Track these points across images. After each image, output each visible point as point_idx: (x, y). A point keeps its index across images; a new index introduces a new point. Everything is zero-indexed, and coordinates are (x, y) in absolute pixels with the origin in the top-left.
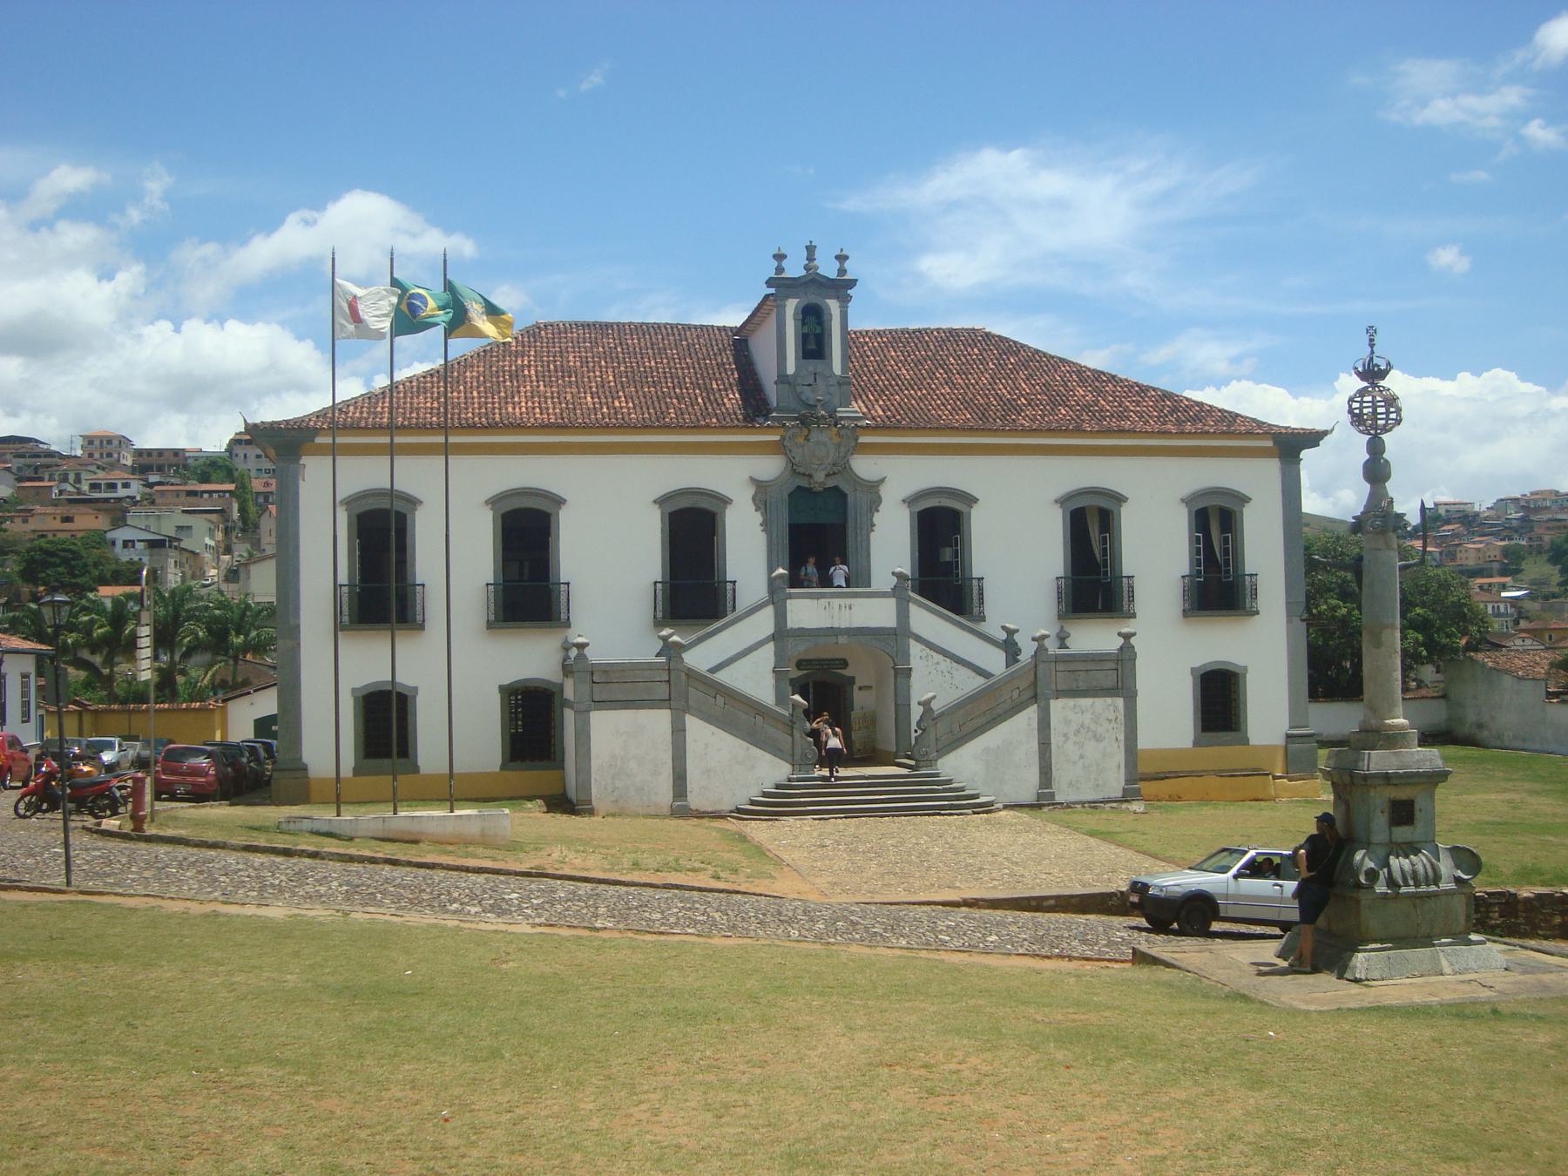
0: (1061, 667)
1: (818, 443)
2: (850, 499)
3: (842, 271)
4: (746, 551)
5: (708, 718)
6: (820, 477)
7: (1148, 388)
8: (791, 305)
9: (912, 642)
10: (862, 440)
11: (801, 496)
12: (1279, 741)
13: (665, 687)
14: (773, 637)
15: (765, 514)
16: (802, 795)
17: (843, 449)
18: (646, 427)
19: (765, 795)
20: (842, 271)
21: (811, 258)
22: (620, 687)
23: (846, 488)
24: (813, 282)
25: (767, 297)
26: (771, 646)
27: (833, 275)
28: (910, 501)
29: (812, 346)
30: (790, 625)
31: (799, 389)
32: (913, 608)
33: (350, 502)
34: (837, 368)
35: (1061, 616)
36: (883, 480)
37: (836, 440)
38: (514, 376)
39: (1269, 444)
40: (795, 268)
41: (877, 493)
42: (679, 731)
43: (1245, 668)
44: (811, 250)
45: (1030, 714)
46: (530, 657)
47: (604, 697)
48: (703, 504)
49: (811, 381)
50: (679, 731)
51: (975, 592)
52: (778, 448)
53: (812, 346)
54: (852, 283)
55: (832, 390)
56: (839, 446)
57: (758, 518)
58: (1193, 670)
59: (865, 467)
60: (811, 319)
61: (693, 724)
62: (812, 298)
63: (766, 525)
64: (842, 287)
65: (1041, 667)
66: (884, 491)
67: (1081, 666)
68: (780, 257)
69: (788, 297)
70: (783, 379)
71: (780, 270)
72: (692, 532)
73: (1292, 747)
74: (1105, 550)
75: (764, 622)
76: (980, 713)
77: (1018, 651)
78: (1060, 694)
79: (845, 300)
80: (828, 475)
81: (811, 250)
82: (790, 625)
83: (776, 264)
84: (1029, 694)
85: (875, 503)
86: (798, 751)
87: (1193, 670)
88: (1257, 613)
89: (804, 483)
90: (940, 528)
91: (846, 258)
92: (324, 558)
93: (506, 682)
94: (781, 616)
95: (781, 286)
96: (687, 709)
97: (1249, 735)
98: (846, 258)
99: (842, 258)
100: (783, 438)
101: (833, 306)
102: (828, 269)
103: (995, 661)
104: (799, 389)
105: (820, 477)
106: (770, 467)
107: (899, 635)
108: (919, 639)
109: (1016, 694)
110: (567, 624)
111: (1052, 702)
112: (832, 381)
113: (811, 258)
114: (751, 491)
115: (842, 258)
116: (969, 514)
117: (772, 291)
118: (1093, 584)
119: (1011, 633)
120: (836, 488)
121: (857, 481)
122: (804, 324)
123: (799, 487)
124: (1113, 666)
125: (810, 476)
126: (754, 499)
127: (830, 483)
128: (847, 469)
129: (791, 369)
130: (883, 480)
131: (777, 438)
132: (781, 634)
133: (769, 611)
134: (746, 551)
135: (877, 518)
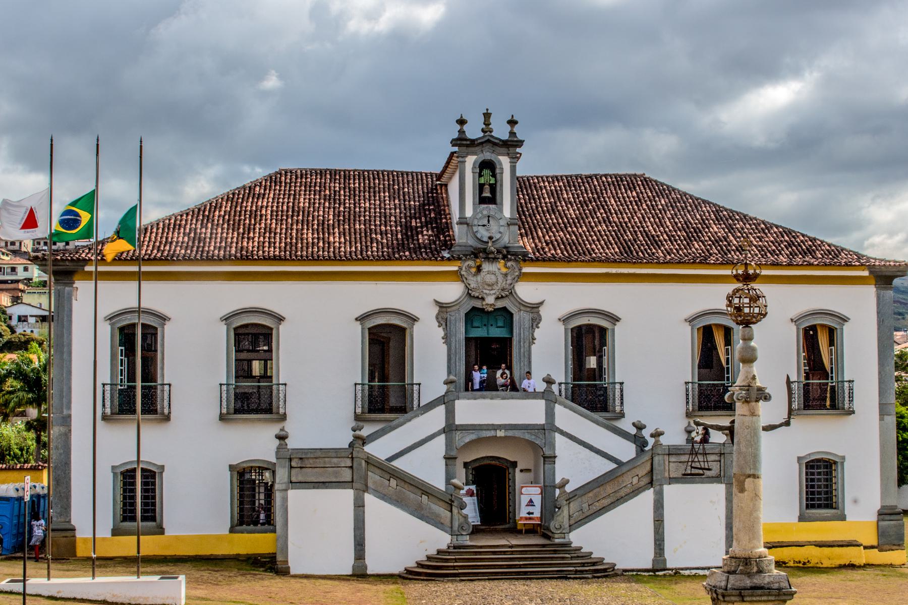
0: (673, 459)
1: (489, 272)
2: (516, 318)
3: (512, 134)
4: (431, 360)
5: (384, 497)
6: (490, 300)
7: (772, 225)
8: (471, 161)
9: (557, 435)
10: (527, 270)
11: (475, 315)
12: (874, 518)
13: (349, 471)
14: (444, 431)
15: (445, 329)
16: (456, 560)
17: (509, 278)
18: (349, 259)
19: (429, 558)
20: (512, 134)
21: (487, 124)
22: (312, 468)
23: (513, 309)
24: (489, 142)
25: (452, 154)
26: (442, 438)
27: (505, 136)
28: (565, 320)
29: (487, 194)
30: (459, 421)
31: (475, 229)
32: (558, 409)
33: (111, 318)
36: (542, 303)
37: (504, 270)
38: (253, 214)
39: (866, 273)
40: (474, 131)
42: (359, 506)
44: (487, 116)
45: (648, 496)
46: (255, 442)
47: (300, 479)
49: (485, 222)
50: (359, 506)
51: (618, 393)
52: (457, 276)
53: (487, 194)
54: (520, 143)
55: (502, 229)
56: (506, 275)
57: (441, 332)
58: (799, 459)
59: (527, 291)
60: (486, 172)
61: (369, 498)
62: (488, 155)
63: (447, 338)
64: (511, 145)
65: (656, 459)
66: (543, 311)
68: (462, 122)
69: (468, 154)
70: (463, 221)
71: (461, 132)
72: (386, 343)
73: (881, 523)
74: (728, 359)
75: (436, 418)
76: (606, 493)
77: (645, 443)
78: (672, 480)
79: (515, 158)
80: (497, 298)
81: (487, 116)
82: (459, 421)
83: (458, 127)
84: (646, 480)
85: (536, 321)
86: (456, 525)
87: (799, 459)
88: (853, 412)
89: (478, 304)
90: (589, 339)
91: (516, 123)
92: (89, 366)
93: (235, 462)
94: (450, 414)
95: (463, 143)
96: (366, 489)
98: (516, 123)
99: (512, 122)
100: (461, 268)
101: (504, 161)
102: (501, 131)
103: (626, 451)
104: (475, 229)
105: (490, 300)
106: (451, 292)
107: (549, 428)
108: (562, 433)
109: (635, 480)
110: (283, 418)
111: (666, 488)
112: (502, 222)
113: (487, 124)
114: (436, 310)
115: (512, 122)
116: (613, 330)
117: (456, 149)
118: (714, 385)
119: (640, 427)
120: (504, 309)
121: (522, 304)
122: (480, 176)
123: (474, 309)
124: (717, 458)
125: (483, 299)
126: (437, 318)
127: (500, 304)
128: (511, 293)
129: (469, 213)
130: (542, 303)
131: (456, 268)
132: (450, 428)
133: (441, 410)
134: (431, 360)
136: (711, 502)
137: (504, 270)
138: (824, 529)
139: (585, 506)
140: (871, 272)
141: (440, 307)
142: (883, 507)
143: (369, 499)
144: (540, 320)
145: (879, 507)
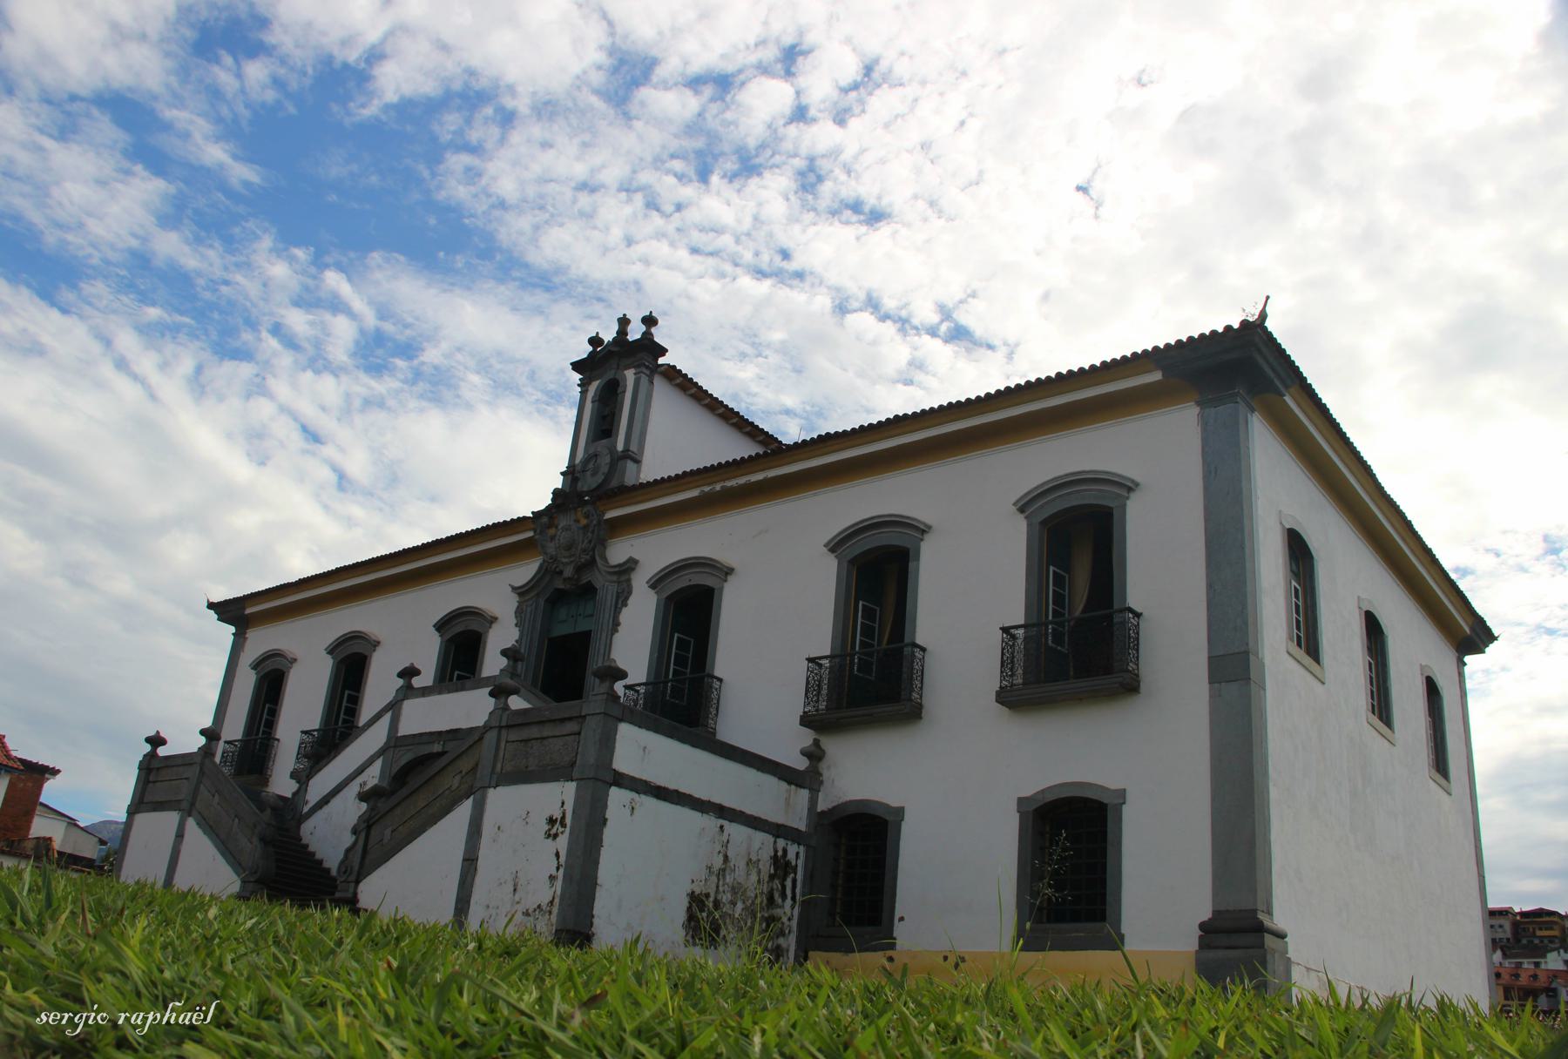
0: (514, 735)
3: (647, 336)
10: (610, 515)
28: (655, 584)
34: (620, 447)
35: (806, 721)
39: (1156, 376)
41: (629, 580)
43: (1122, 794)
44: (624, 322)
48: (474, 625)
58: (1021, 801)
62: (610, 375)
67: (534, 732)
85: (623, 597)
87: (1021, 801)
97: (1124, 929)
99: (650, 321)
101: (630, 375)
115: (650, 321)
116: (721, 589)
125: (561, 572)
131: (531, 534)
132: (395, 742)
135: (626, 615)
136: (552, 821)
137: (584, 522)
138: (1070, 969)
139: (388, 832)
140: (1164, 369)
141: (520, 595)
142: (1217, 913)
143: (191, 823)
144: (630, 593)
145: (1206, 914)
